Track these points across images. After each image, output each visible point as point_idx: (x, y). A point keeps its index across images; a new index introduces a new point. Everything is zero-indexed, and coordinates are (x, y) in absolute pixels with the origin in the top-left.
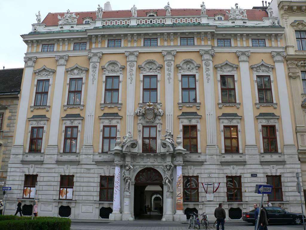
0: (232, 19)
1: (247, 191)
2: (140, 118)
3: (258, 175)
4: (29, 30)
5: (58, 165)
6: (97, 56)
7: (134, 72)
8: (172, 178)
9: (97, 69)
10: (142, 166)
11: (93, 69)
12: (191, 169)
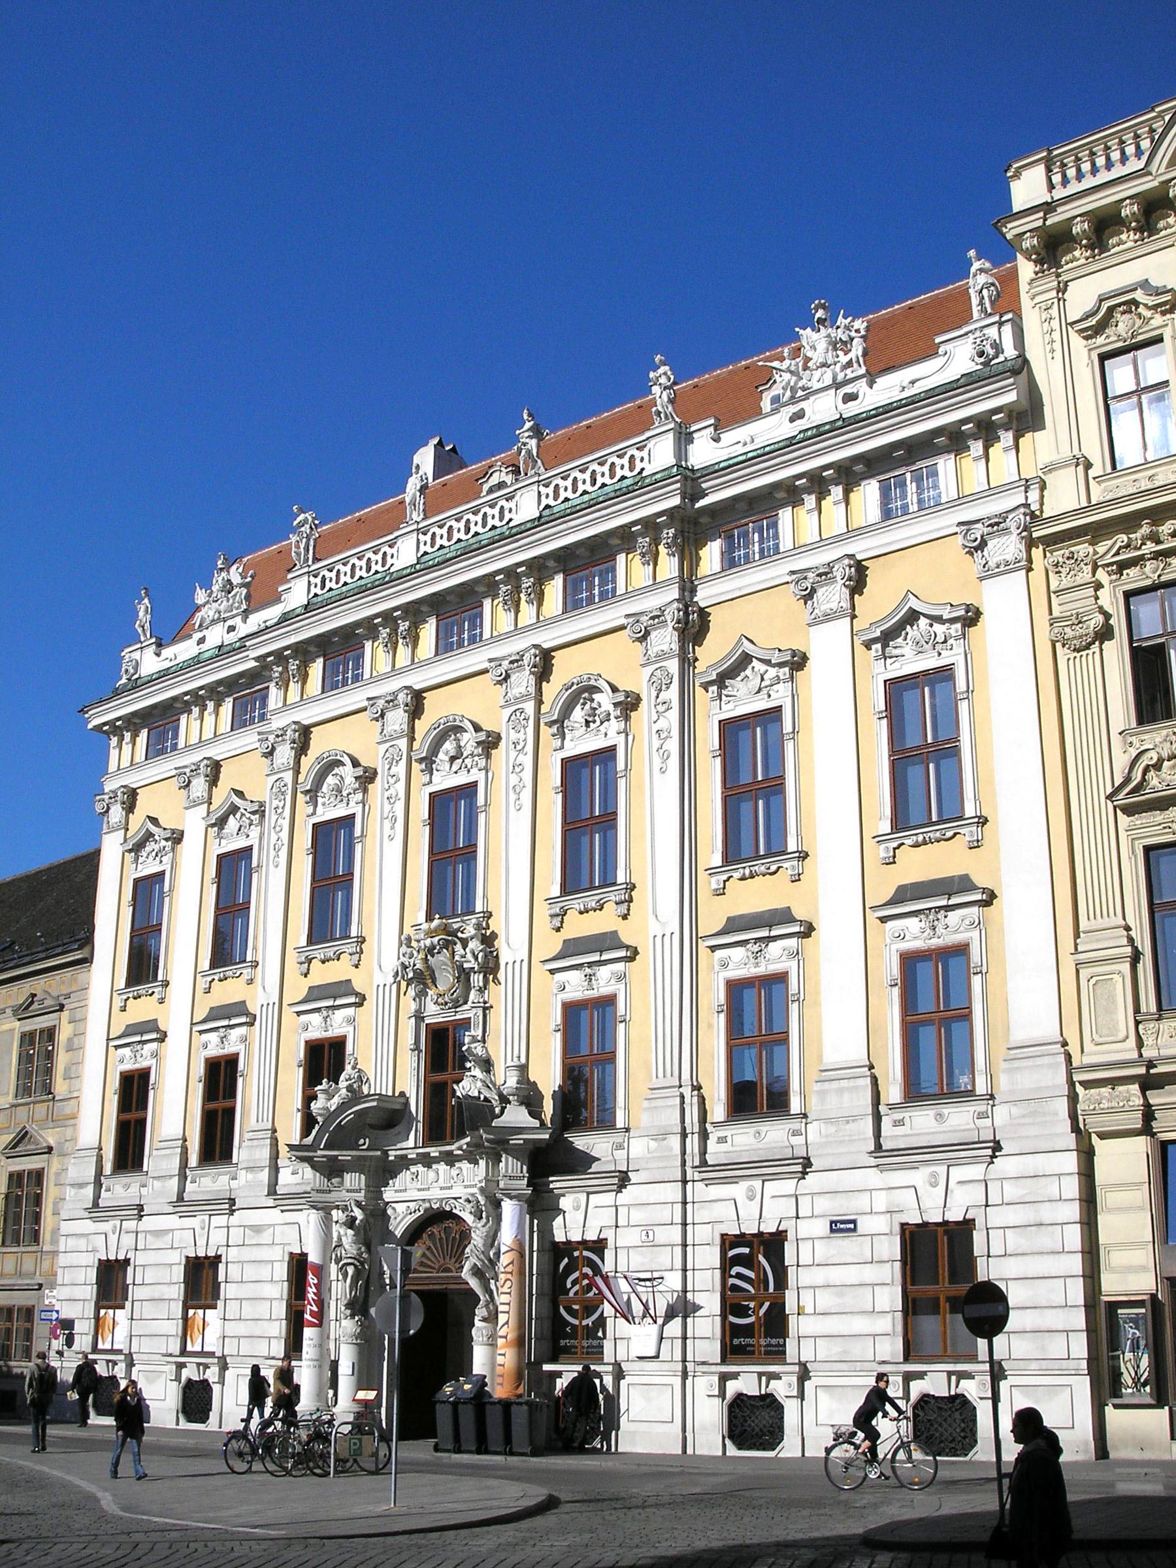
1: (809, 1309)
3: (864, 1225)
11: (275, 803)
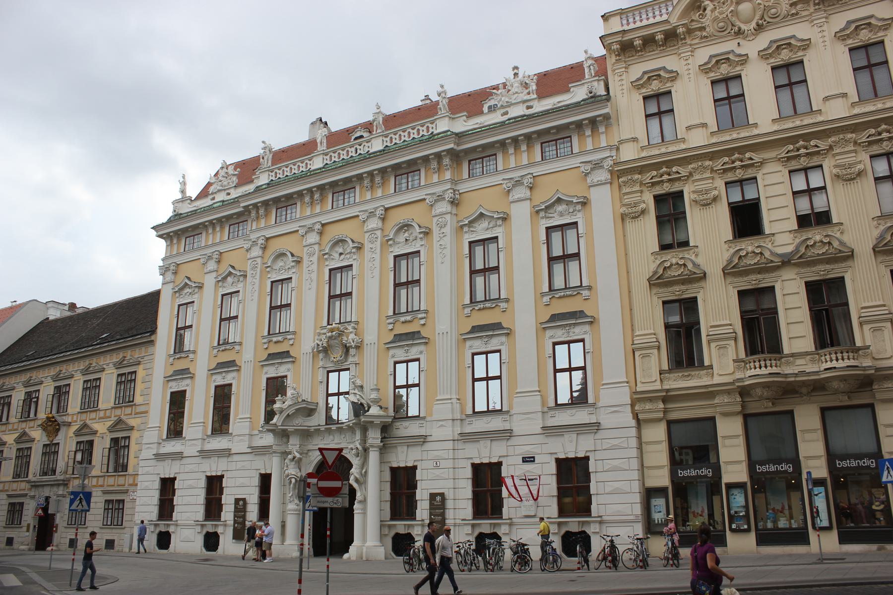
4: (165, 214)
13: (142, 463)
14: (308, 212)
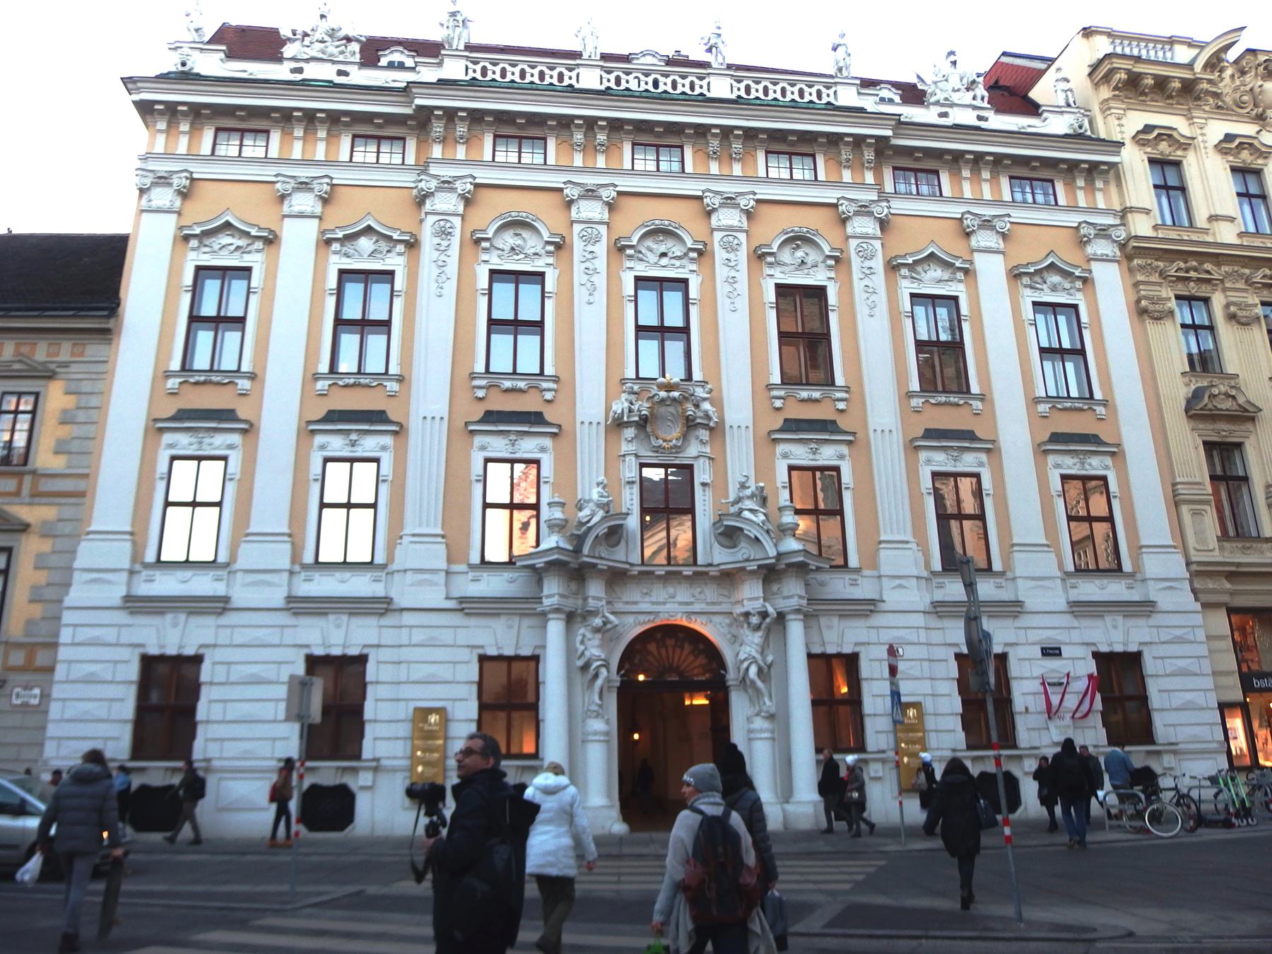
0: (937, 103)
2: (630, 432)
5: (295, 614)
6: (453, 190)
7: (601, 264)
8: (770, 659)
9: (456, 240)
10: (646, 618)
11: (437, 240)
12: (829, 627)
13: (67, 617)
14: (578, 160)
